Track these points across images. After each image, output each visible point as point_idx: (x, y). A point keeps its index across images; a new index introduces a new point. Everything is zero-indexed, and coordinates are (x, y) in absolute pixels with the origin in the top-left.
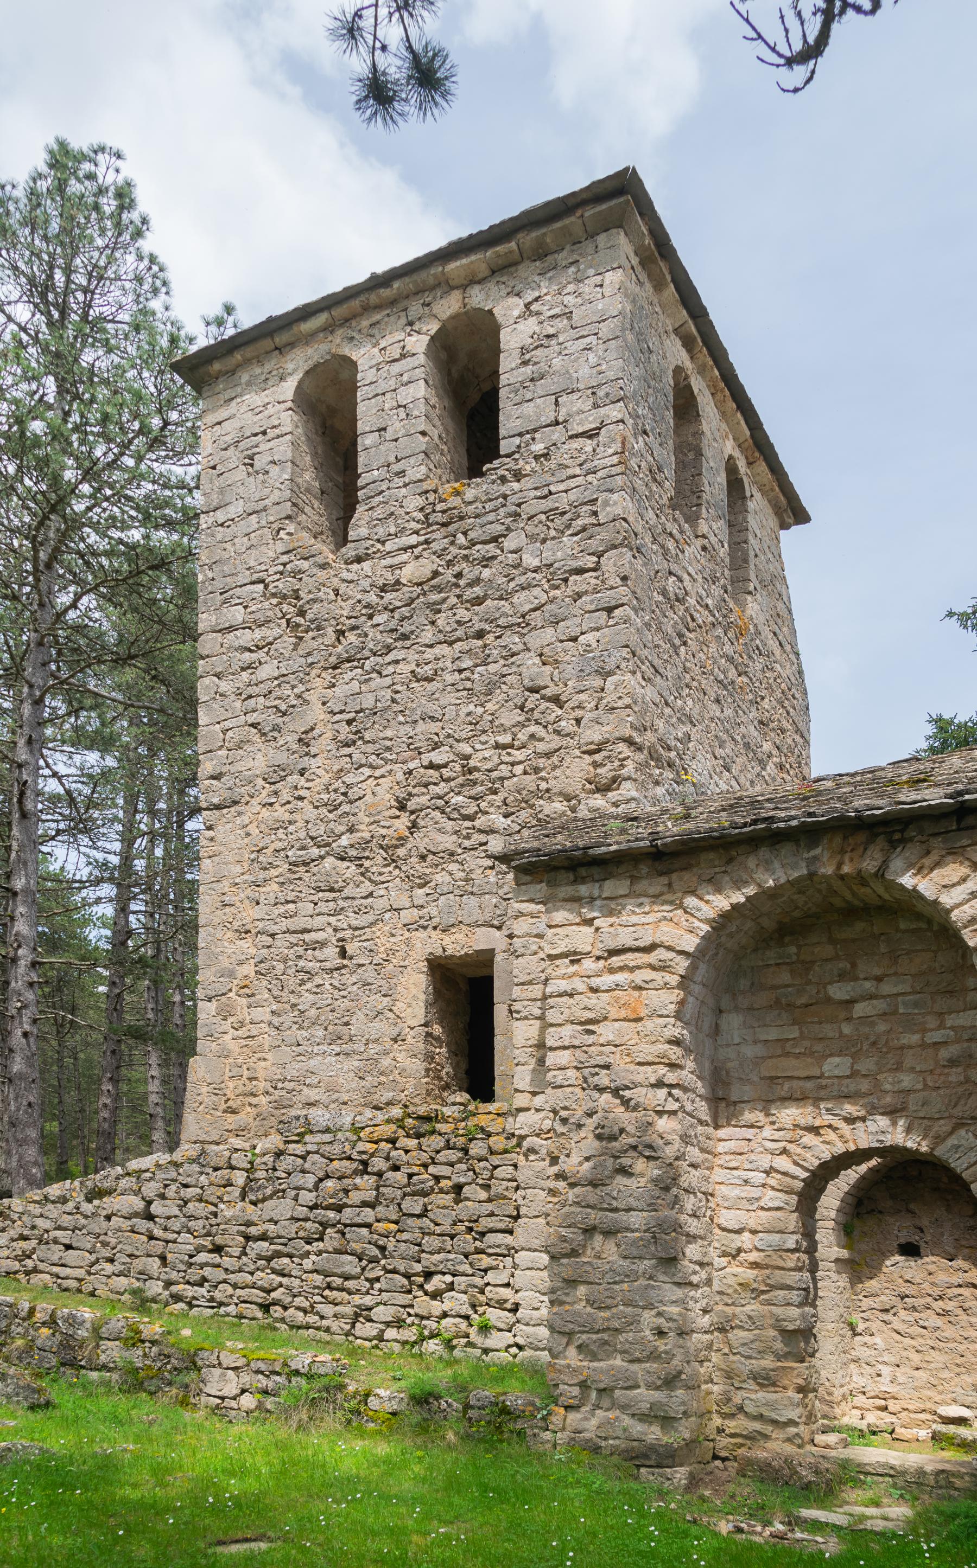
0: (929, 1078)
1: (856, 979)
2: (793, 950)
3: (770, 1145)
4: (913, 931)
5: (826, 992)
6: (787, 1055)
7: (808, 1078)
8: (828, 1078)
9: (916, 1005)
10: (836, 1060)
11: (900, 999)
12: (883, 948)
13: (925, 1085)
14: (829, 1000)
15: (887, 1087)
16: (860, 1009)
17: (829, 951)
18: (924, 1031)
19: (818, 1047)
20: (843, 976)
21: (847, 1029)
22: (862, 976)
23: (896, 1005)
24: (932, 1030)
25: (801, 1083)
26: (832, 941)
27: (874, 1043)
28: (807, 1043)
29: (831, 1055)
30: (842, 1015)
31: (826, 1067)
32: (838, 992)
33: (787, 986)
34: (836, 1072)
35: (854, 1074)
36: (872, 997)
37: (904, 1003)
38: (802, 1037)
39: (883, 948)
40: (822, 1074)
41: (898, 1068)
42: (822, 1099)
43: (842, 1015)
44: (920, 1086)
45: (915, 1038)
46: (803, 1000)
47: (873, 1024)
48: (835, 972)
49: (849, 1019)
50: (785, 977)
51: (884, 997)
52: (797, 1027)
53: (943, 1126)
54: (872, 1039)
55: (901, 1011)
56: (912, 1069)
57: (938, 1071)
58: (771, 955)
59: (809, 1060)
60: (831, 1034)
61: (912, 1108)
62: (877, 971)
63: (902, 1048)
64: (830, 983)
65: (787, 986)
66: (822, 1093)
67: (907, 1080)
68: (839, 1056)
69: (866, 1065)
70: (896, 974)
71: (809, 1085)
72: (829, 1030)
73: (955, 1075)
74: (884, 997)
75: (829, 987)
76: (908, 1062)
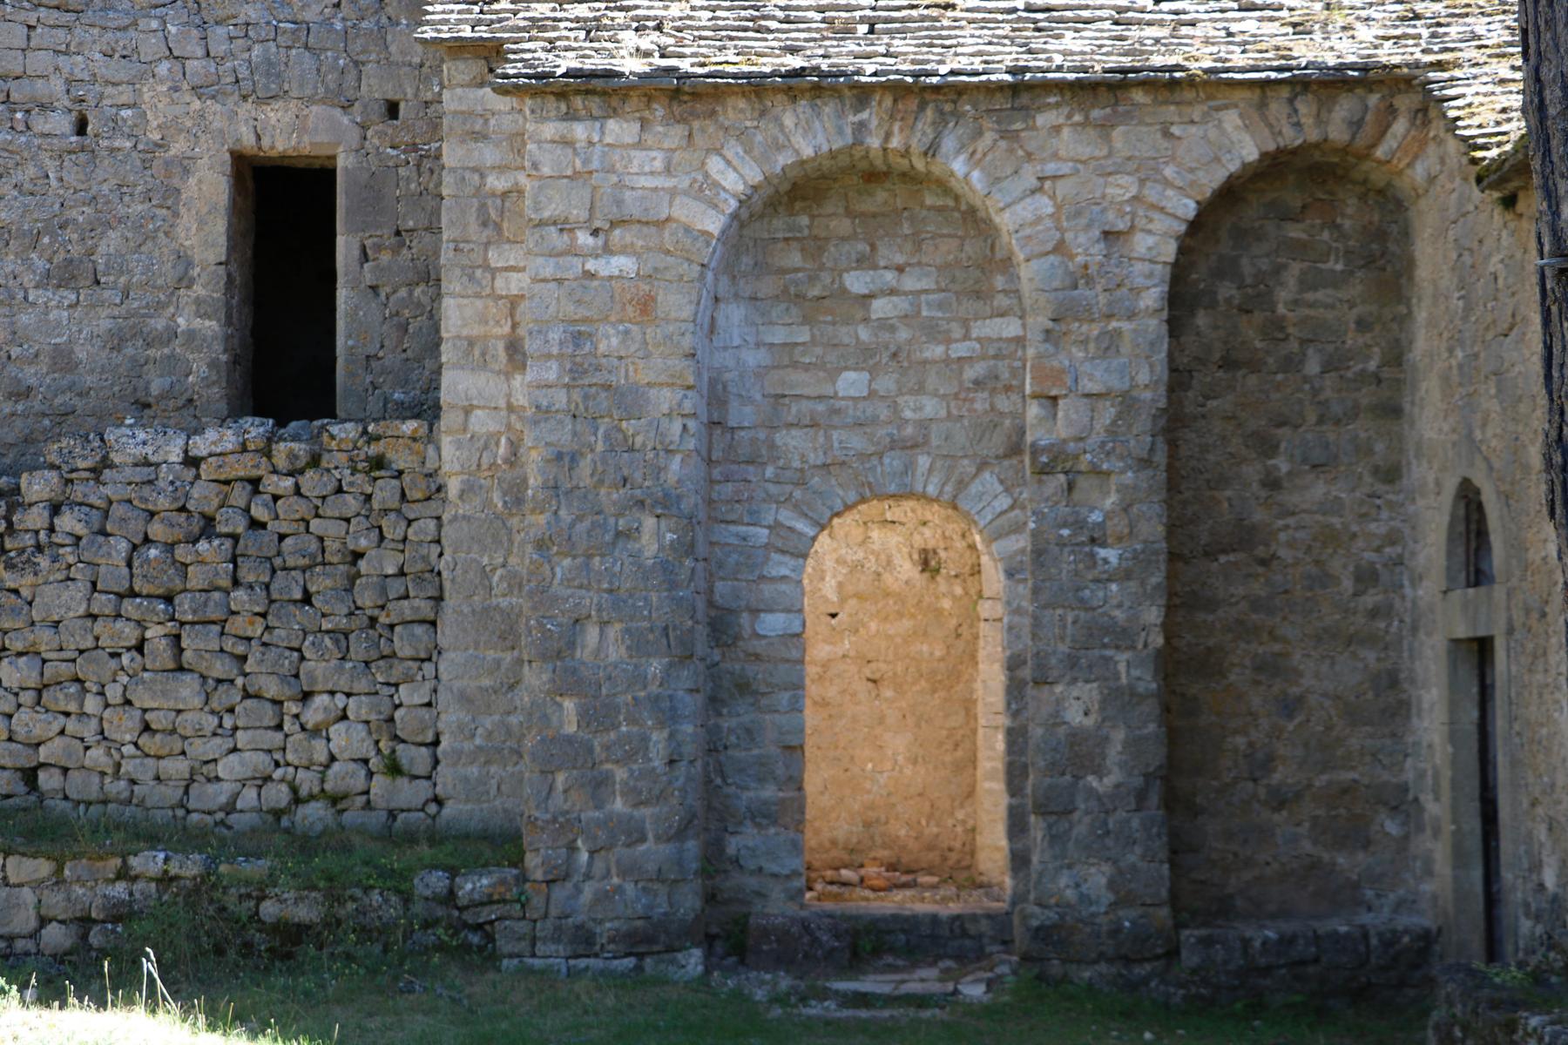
0: (953, 404)
1: (875, 267)
2: (804, 220)
3: (773, 489)
4: (940, 210)
5: (841, 283)
6: (795, 365)
7: (820, 398)
8: (843, 398)
9: (940, 306)
10: (851, 375)
11: (923, 297)
12: (906, 229)
13: (949, 412)
14: (844, 291)
15: (908, 414)
16: (880, 307)
17: (843, 226)
18: (948, 341)
19: (832, 357)
20: (865, 262)
21: (864, 334)
22: (882, 263)
23: (919, 306)
24: (957, 341)
25: (810, 404)
26: (849, 213)
27: (895, 355)
28: (819, 350)
29: (847, 368)
30: (860, 315)
31: (840, 384)
32: (856, 282)
33: (797, 270)
34: (852, 393)
35: (872, 394)
36: (893, 292)
37: (928, 304)
38: (813, 342)
39: (906, 229)
40: (836, 393)
41: (920, 389)
42: (836, 428)
43: (860, 315)
44: (943, 413)
45: (938, 351)
46: (815, 292)
47: (892, 329)
48: (854, 257)
49: (866, 320)
50: (795, 258)
51: (906, 294)
52: (807, 327)
53: (968, 466)
54: (893, 348)
55: (924, 313)
56: (935, 394)
57: (963, 395)
58: (779, 224)
59: (821, 374)
60: (846, 340)
61: (935, 442)
62: (900, 259)
63: (925, 362)
64: (847, 270)
65: (797, 270)
66: (836, 420)
67: (931, 407)
68: (855, 370)
69: (886, 384)
70: (919, 263)
71: (821, 407)
72: (844, 334)
73: (981, 402)
74: (906, 294)
75: (845, 275)
76: (932, 381)
